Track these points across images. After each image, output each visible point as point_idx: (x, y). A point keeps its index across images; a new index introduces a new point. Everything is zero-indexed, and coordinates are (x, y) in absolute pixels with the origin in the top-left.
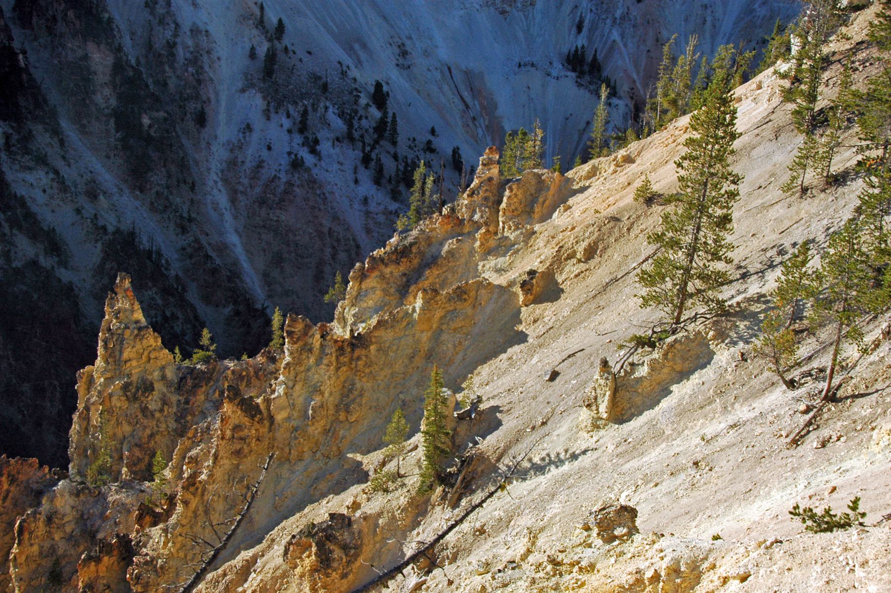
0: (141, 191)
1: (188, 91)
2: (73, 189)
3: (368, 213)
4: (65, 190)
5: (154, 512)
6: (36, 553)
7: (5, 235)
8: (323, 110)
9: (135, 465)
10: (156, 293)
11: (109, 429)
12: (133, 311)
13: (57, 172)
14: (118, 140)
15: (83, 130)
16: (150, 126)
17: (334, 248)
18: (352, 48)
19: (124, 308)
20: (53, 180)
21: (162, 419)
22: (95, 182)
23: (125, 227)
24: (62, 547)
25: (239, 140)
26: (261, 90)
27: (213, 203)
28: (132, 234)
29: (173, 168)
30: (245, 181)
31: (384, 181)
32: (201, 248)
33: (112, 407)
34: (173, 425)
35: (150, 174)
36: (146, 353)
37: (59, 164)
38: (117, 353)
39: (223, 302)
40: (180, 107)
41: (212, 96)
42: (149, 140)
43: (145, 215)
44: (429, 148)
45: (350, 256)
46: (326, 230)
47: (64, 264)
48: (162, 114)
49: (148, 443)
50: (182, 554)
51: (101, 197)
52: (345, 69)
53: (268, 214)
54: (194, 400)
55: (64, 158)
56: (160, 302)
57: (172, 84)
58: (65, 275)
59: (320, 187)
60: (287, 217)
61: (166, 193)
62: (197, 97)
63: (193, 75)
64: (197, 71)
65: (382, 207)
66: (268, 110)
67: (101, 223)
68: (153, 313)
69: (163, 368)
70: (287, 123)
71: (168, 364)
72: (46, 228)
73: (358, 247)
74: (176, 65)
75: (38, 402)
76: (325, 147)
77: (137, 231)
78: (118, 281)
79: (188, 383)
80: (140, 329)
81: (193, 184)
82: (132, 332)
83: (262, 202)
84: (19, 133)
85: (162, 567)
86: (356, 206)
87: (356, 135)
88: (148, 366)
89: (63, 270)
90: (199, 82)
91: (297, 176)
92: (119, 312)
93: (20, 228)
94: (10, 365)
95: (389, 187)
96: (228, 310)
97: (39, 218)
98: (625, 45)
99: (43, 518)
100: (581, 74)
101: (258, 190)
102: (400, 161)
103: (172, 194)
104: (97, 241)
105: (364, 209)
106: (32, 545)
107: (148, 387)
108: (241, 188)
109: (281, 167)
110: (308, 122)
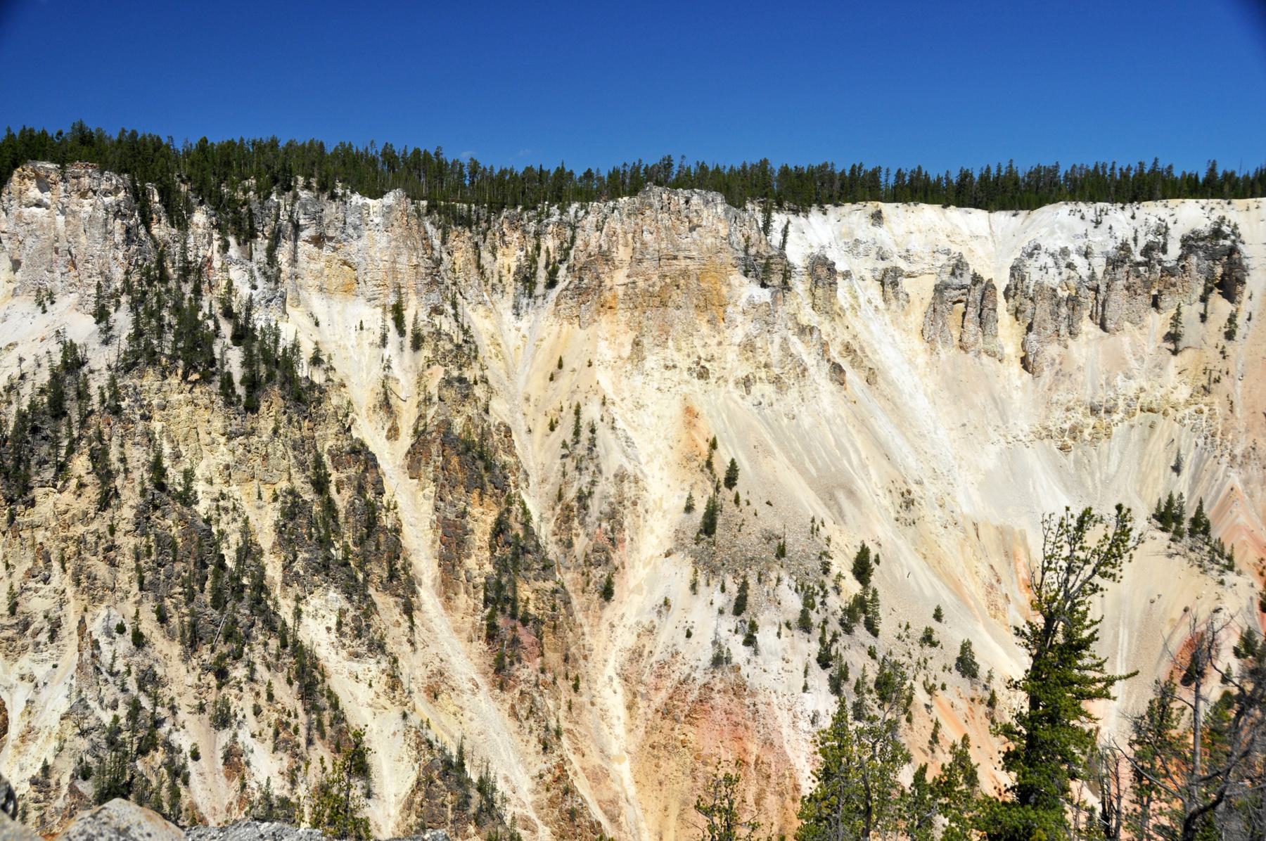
0: (502, 689)
8: (775, 581)
18: (832, 497)
20: (383, 671)
22: (442, 674)
26: (693, 554)
29: (553, 658)
44: (928, 639)
46: (751, 759)
48: (550, 585)
53: (673, 729)
55: (409, 641)
59: (753, 694)
64: (612, 531)
70: (720, 600)
76: (765, 637)
77: (467, 747)
81: (577, 679)
83: (666, 712)
87: (815, 618)
93: (323, 736)
98: (1251, 496)
100: (1178, 534)
108: (642, 689)
109: (700, 664)
110: (751, 599)
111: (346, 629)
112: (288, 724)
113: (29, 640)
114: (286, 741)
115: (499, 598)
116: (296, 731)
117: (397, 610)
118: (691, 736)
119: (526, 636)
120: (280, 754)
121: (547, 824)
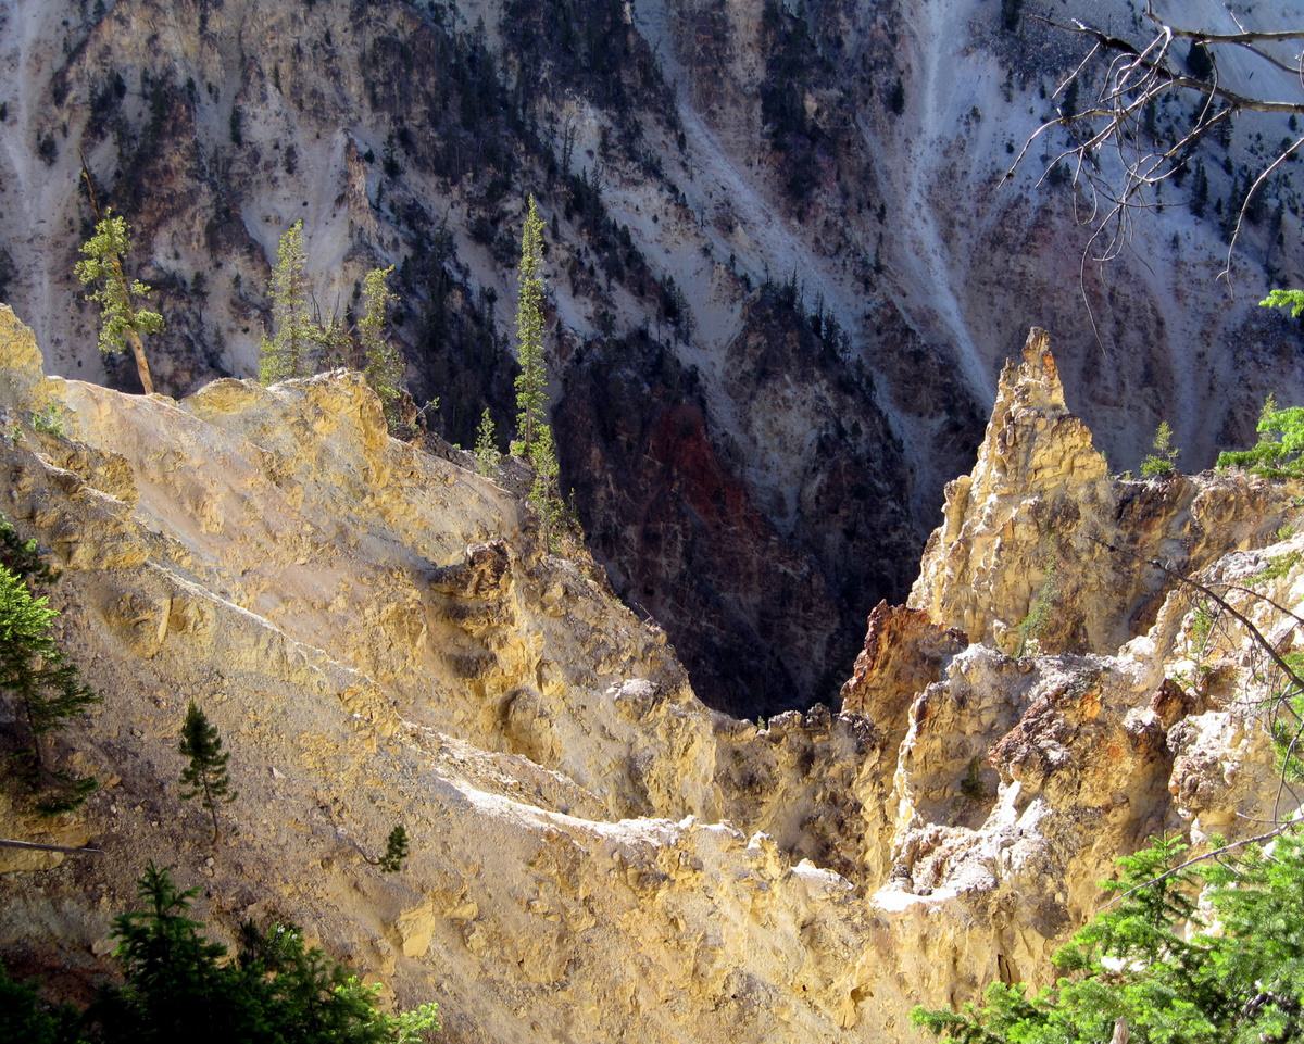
0: (801, 220)
1: (875, 54)
2: (698, 217)
3: (1178, 264)
4: (687, 218)
5: (1183, 694)
6: (938, 751)
7: (599, 288)
9: (1052, 633)
10: (828, 389)
11: (1010, 577)
12: (1051, 390)
13: (674, 189)
14: (766, 136)
15: (712, 120)
16: (818, 112)
17: (1118, 322)
19: (1032, 386)
21: (1092, 564)
23: (780, 278)
24: (975, 745)
25: (959, 136)
26: (997, 51)
27: (913, 242)
28: (791, 292)
29: (851, 183)
30: (969, 205)
31: (1207, 208)
32: (895, 316)
33: (1015, 541)
34: (1109, 575)
35: (816, 191)
36: (1068, 459)
37: (678, 177)
38: (1022, 457)
39: (931, 408)
40: (863, 80)
41: (914, 64)
42: (815, 135)
43: (806, 260)
45: (1146, 337)
46: (1105, 292)
47: (684, 336)
48: (835, 93)
49: (1073, 599)
50: (1262, 757)
51: (739, 228)
52: (1138, 13)
54: (1146, 536)
55: (684, 165)
56: (831, 403)
57: (850, 42)
58: (685, 355)
60: (1038, 267)
61: (840, 223)
62: (891, 62)
63: (884, 27)
64: (891, 21)
65: (1203, 255)
66: (1009, 85)
67: (740, 271)
68: (821, 420)
69: (1092, 483)
71: (1100, 477)
72: (658, 278)
73: (1160, 323)
74: (857, 12)
75: (649, 557)
77: (799, 284)
78: (1030, 340)
79: (1133, 510)
80: (1061, 419)
81: (883, 208)
82: (1049, 423)
83: (997, 241)
84: (621, 126)
85: (1233, 775)
86: (1158, 251)
87: (1160, 128)
88: (1069, 479)
89: (681, 346)
90: (894, 38)
91: (1057, 196)
92: (1027, 391)
93: (621, 279)
94: (610, 496)
95: (1216, 220)
96: (938, 423)
97: (648, 262)
99: (951, 698)
101: (990, 220)
102: (1236, 173)
103: (849, 225)
104: (734, 300)
105: (1172, 257)
106: (933, 737)
107: (1070, 513)
108: (960, 217)
111: (612, 152)
112: (582, 264)
113: (262, 175)
114: (586, 283)
115: (779, 107)
116: (592, 271)
117: (660, 129)
118: (1031, 268)
119: (823, 161)
120: (583, 299)
121: (883, 370)
